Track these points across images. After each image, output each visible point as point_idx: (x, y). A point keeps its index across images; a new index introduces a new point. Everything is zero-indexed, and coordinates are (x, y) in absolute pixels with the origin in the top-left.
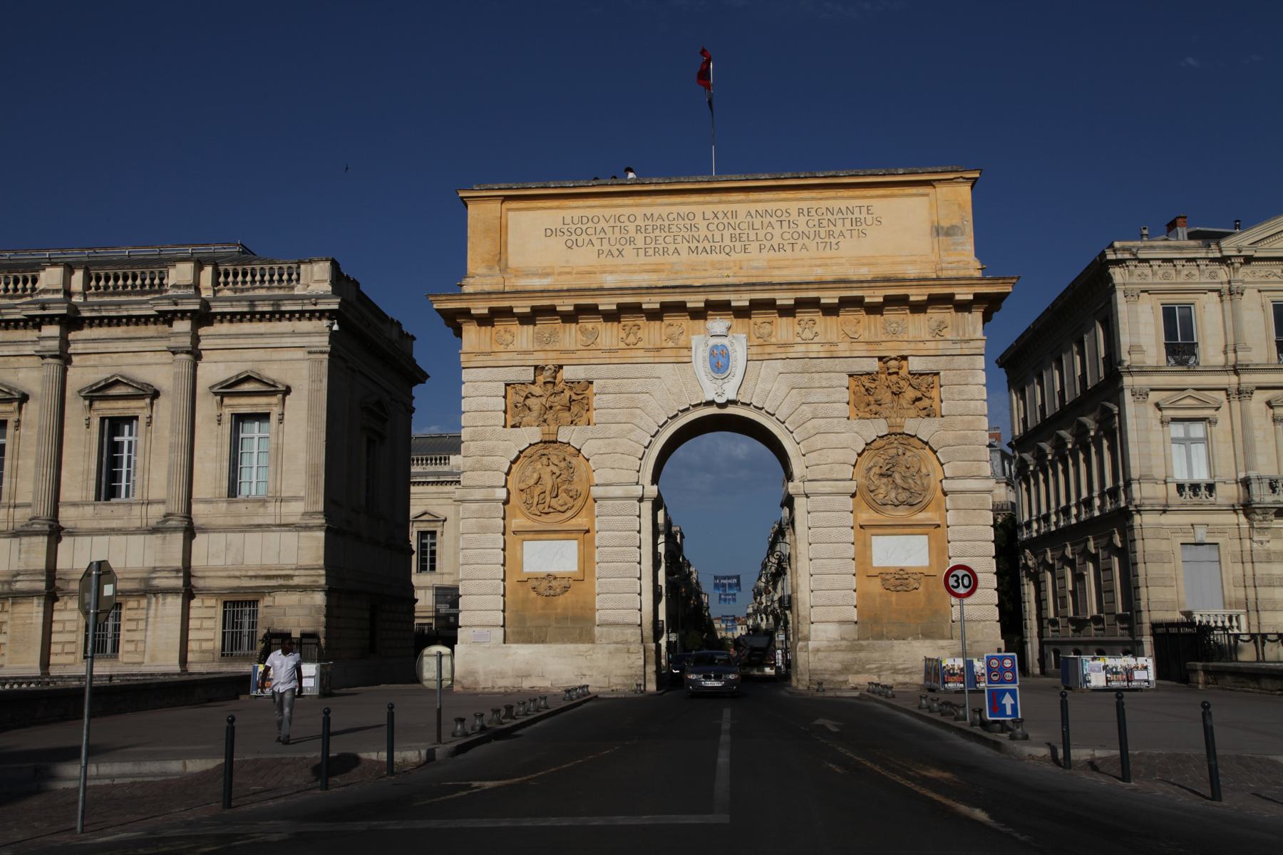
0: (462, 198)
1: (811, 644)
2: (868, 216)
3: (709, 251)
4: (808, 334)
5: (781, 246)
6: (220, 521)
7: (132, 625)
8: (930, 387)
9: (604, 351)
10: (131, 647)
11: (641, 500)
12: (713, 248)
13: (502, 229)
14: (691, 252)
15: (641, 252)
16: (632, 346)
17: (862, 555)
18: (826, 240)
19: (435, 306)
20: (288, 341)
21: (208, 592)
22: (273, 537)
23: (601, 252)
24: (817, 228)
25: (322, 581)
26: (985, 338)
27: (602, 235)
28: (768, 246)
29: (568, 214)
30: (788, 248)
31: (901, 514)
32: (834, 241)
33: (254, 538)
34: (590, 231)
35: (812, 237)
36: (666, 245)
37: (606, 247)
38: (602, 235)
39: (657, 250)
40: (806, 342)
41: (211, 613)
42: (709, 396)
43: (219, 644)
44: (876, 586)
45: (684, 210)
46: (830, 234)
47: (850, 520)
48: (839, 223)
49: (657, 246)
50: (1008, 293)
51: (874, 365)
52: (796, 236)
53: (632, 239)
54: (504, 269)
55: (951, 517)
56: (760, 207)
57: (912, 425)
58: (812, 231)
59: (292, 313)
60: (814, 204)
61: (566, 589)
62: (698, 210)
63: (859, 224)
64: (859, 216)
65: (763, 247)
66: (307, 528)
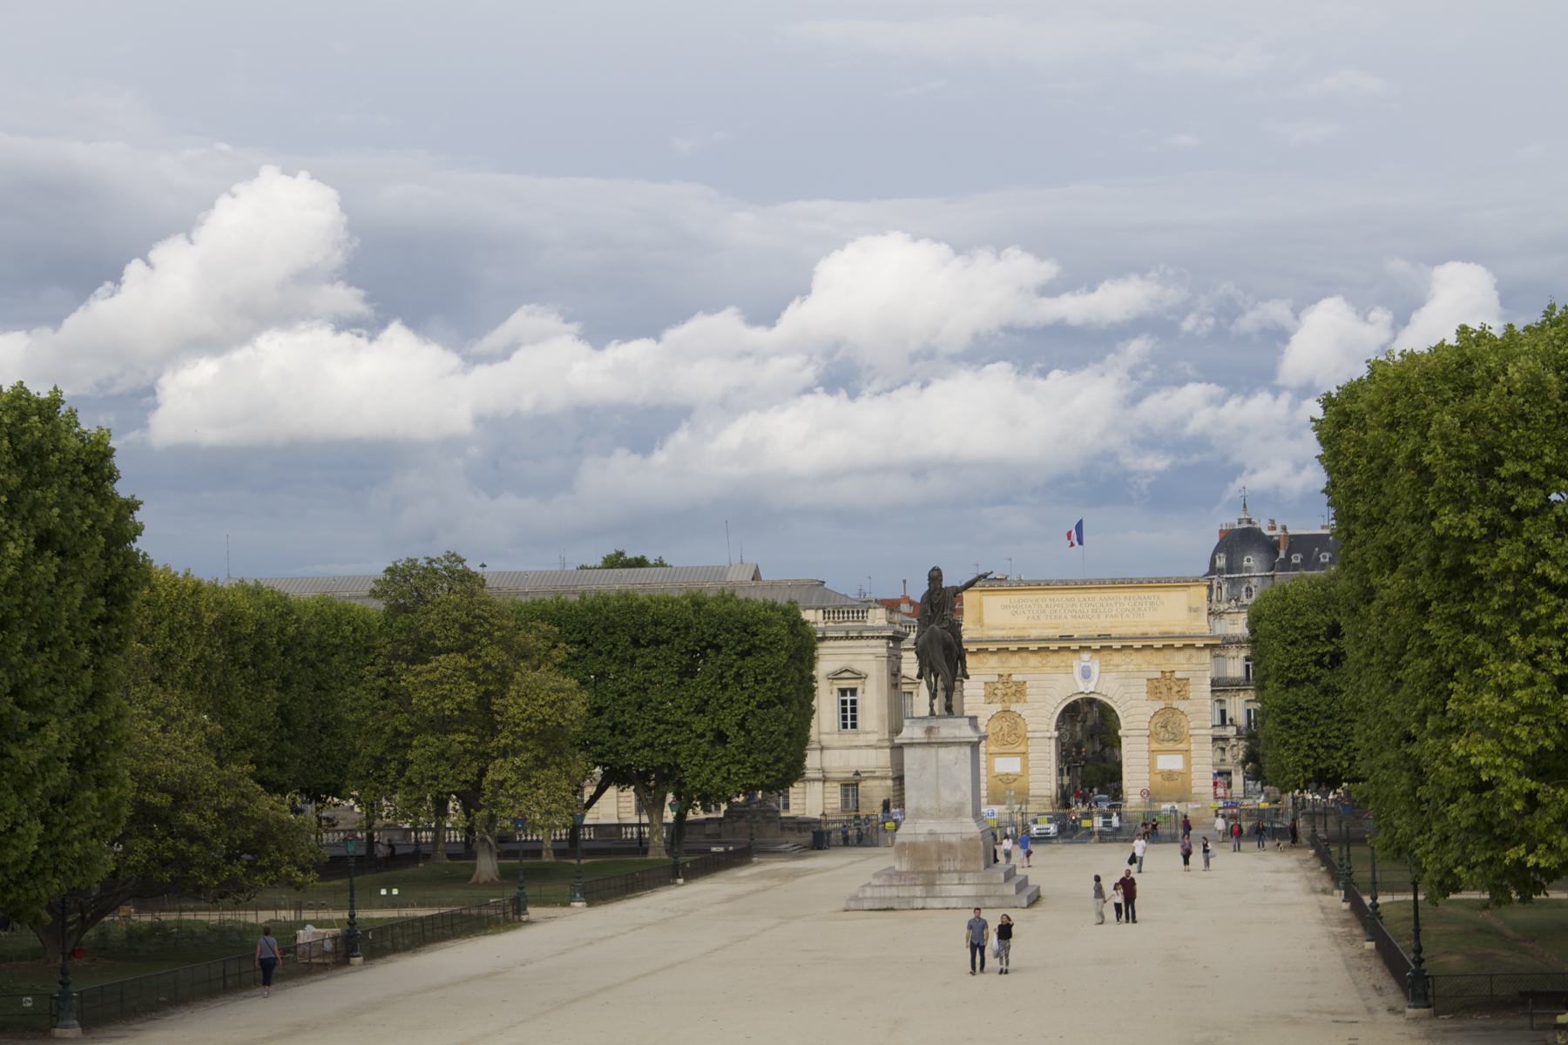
1: (1128, 805)
4: (1128, 660)
6: (836, 744)
7: (796, 796)
8: (1185, 685)
10: (796, 807)
11: (1050, 738)
13: (981, 605)
17: (1152, 764)
20: (865, 651)
21: (834, 780)
22: (864, 752)
25: (890, 774)
29: (1012, 597)
31: (1170, 745)
33: (854, 752)
37: (1031, 615)
40: (1128, 664)
41: (834, 790)
42: (1081, 690)
43: (840, 805)
44: (1159, 778)
45: (1070, 596)
47: (1147, 747)
51: (1159, 675)
54: (982, 626)
55: (1192, 747)
56: (1106, 595)
57: (1176, 704)
59: (867, 637)
60: (1133, 594)
61: (1015, 780)
62: (1076, 596)
66: (881, 747)
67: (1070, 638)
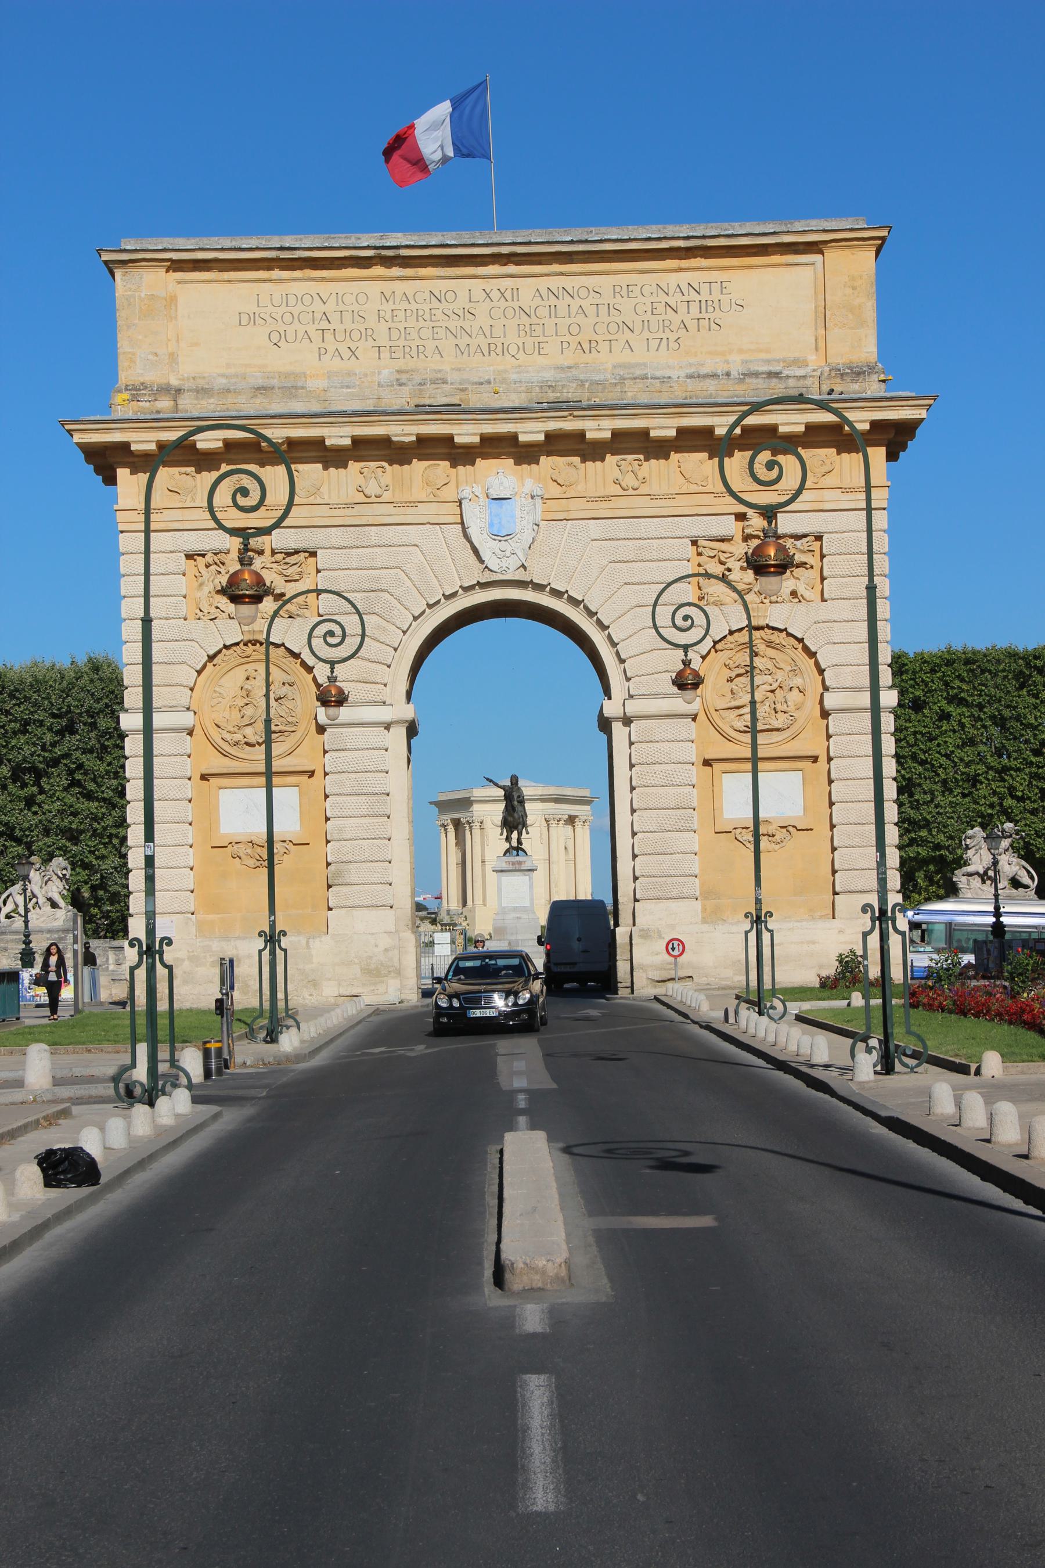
0: (106, 263)
2: (722, 297)
3: (486, 353)
5: (594, 344)
9: (332, 506)
12: (493, 347)
14: (459, 353)
15: (386, 354)
16: (373, 499)
18: (660, 335)
19: (77, 438)
23: (323, 351)
24: (648, 316)
26: (889, 484)
27: (324, 325)
28: (573, 346)
30: (604, 347)
32: (673, 337)
34: (306, 318)
35: (637, 328)
36: (419, 342)
38: (324, 325)
39: (407, 349)
46: (666, 326)
47: (692, 753)
48: (682, 308)
49: (406, 343)
50: (922, 420)
52: (613, 328)
53: (370, 332)
58: (638, 320)
63: (711, 309)
64: (709, 298)
65: (565, 345)
67: (453, 410)
